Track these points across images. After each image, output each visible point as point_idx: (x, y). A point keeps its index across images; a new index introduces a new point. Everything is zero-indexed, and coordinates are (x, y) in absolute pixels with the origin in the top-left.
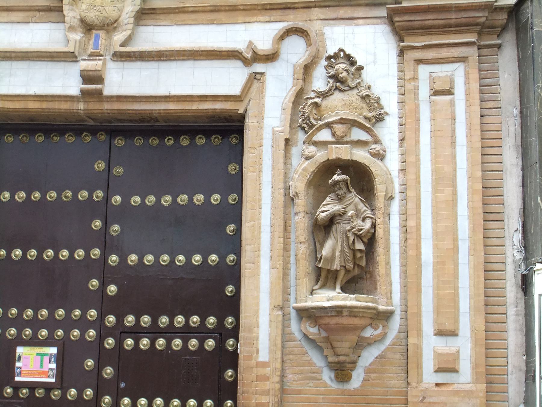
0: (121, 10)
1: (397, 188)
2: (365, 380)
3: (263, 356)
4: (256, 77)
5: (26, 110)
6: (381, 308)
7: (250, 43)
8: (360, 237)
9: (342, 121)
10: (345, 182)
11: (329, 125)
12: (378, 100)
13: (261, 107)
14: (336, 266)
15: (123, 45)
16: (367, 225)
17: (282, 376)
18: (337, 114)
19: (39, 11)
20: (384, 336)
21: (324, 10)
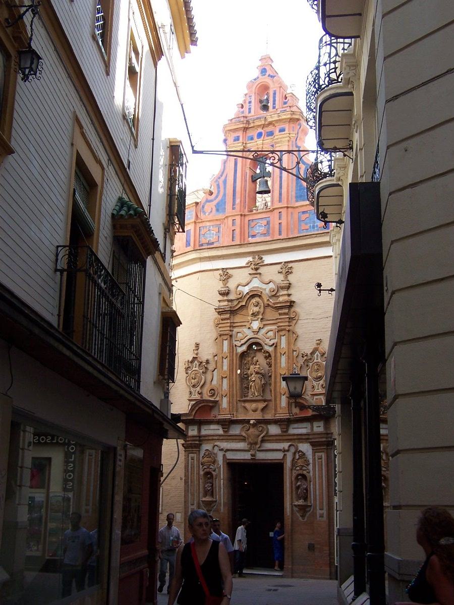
12: (308, 460)
13: (286, 461)
20: (310, 510)
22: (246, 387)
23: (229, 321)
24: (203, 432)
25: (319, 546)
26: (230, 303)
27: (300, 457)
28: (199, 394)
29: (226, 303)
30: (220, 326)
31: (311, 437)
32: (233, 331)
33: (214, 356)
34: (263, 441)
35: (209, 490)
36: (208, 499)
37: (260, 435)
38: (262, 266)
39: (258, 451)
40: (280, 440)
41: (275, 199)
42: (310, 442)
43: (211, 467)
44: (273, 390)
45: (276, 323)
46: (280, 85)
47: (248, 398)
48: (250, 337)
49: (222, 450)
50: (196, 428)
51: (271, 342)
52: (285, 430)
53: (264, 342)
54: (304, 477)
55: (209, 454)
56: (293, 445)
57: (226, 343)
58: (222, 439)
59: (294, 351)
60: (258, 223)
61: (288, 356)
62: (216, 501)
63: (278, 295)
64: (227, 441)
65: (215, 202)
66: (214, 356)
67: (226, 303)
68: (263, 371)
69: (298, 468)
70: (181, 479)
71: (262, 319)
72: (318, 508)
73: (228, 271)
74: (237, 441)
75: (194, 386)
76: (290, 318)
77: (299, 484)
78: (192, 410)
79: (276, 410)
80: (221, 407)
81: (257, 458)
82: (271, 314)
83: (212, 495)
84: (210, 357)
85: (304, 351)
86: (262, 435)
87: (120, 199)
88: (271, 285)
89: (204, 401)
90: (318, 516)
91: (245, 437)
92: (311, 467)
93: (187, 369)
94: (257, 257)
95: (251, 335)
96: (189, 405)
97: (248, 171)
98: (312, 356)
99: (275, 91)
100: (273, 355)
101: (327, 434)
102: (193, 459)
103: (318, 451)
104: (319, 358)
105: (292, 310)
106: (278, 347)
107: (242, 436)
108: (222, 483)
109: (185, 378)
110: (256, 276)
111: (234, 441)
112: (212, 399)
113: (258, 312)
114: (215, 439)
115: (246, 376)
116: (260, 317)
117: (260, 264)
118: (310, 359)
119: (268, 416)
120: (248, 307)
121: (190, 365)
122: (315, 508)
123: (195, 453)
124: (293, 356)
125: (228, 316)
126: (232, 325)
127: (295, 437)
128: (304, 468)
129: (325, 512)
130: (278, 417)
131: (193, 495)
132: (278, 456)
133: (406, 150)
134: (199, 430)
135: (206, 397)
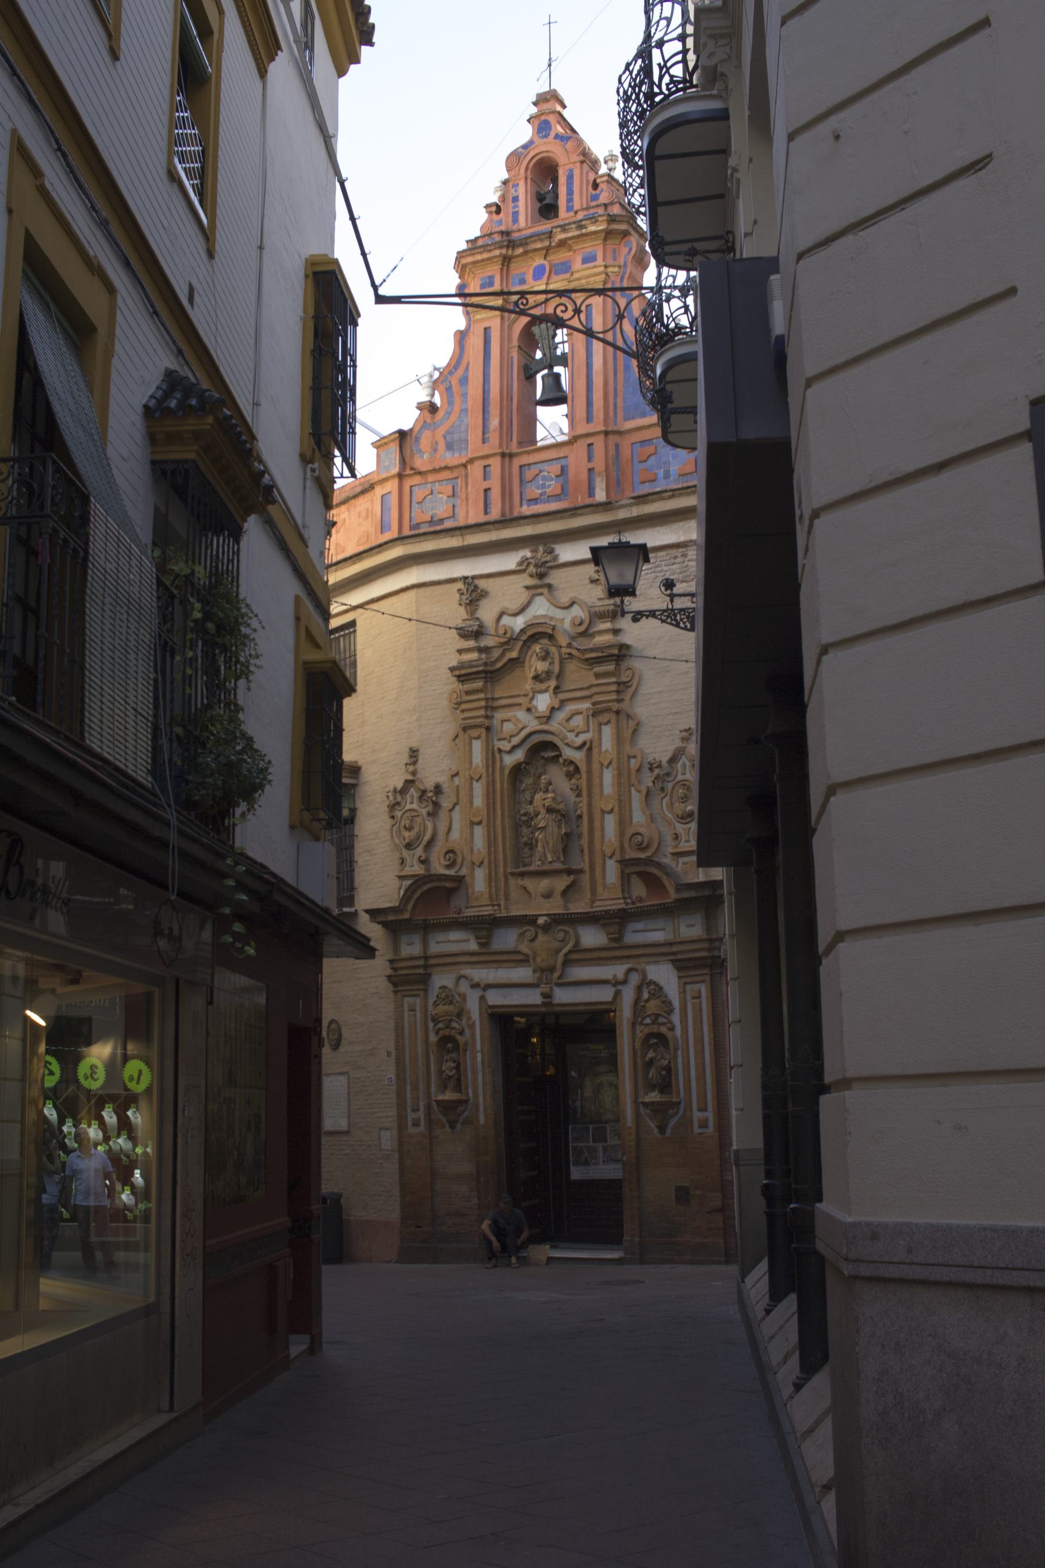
0: (556, 961)
1: (680, 1044)
4: (618, 993)
6: (674, 1100)
7: (615, 976)
8: (663, 1069)
9: (653, 1014)
10: (656, 1043)
11: (648, 1016)
12: (670, 1002)
14: (654, 1082)
15: (559, 978)
16: (666, 1062)
17: (637, 1133)
20: (677, 1112)
22: (526, 844)
23: (482, 696)
24: (434, 948)
26: (484, 656)
27: (652, 996)
28: (422, 862)
29: (475, 656)
30: (463, 706)
31: (675, 949)
32: (493, 717)
33: (453, 776)
34: (567, 962)
35: (450, 1077)
36: (449, 1096)
37: (560, 950)
38: (551, 568)
39: (559, 985)
41: (578, 416)
42: (673, 962)
44: (586, 851)
45: (590, 697)
46: (582, 158)
47: (532, 868)
48: (533, 729)
49: (475, 986)
50: (417, 939)
51: (579, 741)
52: (617, 936)
53: (562, 740)
54: (662, 1039)
55: (446, 997)
56: (635, 970)
57: (477, 746)
59: (629, 757)
60: (541, 471)
61: (619, 769)
62: (466, 1101)
63: (591, 631)
65: (442, 431)
66: (453, 776)
67: (475, 656)
68: (561, 806)
69: (648, 1021)
70: (389, 1054)
71: (557, 688)
73: (476, 582)
74: (509, 965)
75: (409, 846)
76: (619, 684)
77: (651, 1054)
78: (405, 899)
79: (593, 892)
80: (470, 890)
81: (556, 1001)
82: (578, 676)
83: (458, 1087)
84: (442, 779)
85: (656, 756)
86: (565, 950)
87: (169, 374)
88: (577, 612)
89: (429, 878)
90: (696, 1125)
91: (525, 955)
92: (676, 1018)
93: (392, 807)
94: (541, 549)
95: (534, 725)
96: (400, 888)
97: (515, 354)
98: (673, 768)
99: (571, 171)
100: (583, 768)
101: (711, 941)
102: (412, 1010)
104: (688, 772)
105: (624, 665)
106: (595, 751)
107: (519, 952)
108: (479, 1059)
109: (388, 826)
110: (539, 591)
111: (505, 965)
112: (451, 872)
113: (548, 673)
115: (524, 818)
116: (553, 683)
117: (548, 565)
118: (668, 774)
119: (579, 907)
120: (524, 662)
121: (399, 799)
122: (689, 1108)
123: (418, 996)
124: (629, 770)
125: (479, 684)
126: (490, 703)
128: (661, 1020)
129: (710, 1115)
130: (600, 906)
131: (415, 1088)
132: (604, 995)
133: (837, 137)
134: (425, 944)
135: (438, 867)
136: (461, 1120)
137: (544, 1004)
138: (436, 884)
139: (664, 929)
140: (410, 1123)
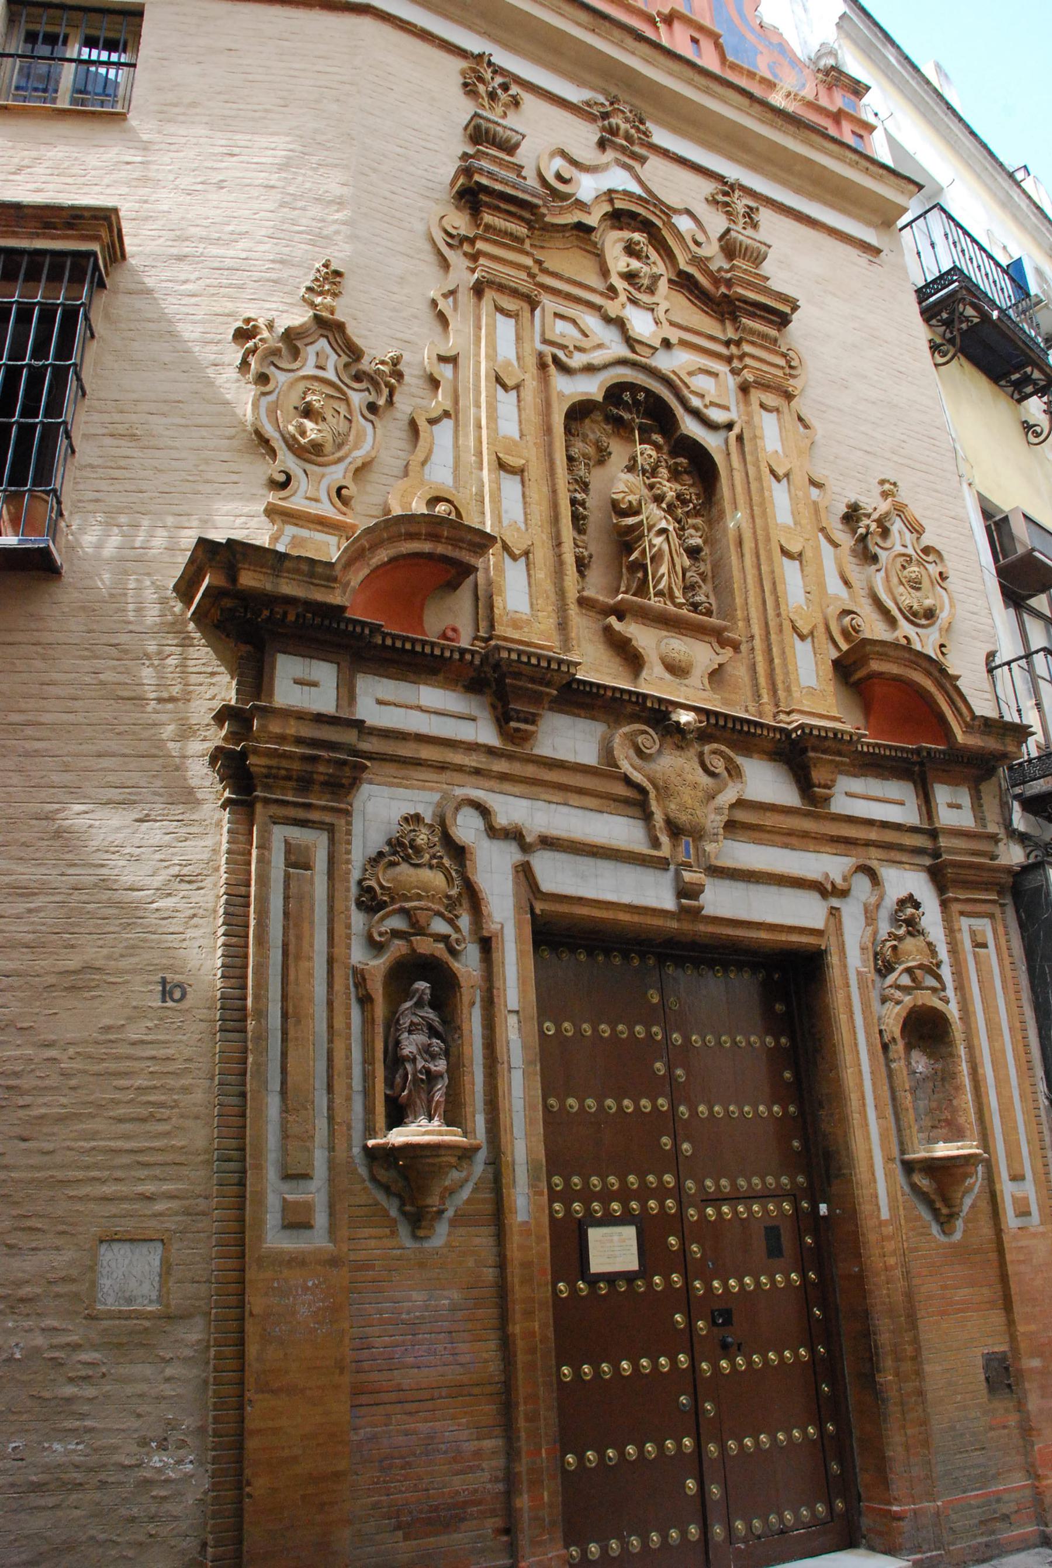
2: (964, 1231)
3: (885, 1214)
5: (616, 922)
7: (827, 875)
18: (914, 960)
19: (615, 800)
21: (880, 850)
25: (1036, 1363)
40: (805, 835)
43: (440, 926)
50: (325, 673)
58: (504, 777)
64: (536, 790)
72: (1004, 1175)
103: (968, 908)
111: (574, 799)
114: (460, 769)
127: (873, 835)
134: (347, 692)
136: (450, 1213)
137: (683, 910)
138: (440, 549)
139: (902, 804)
140: (272, 1219)
